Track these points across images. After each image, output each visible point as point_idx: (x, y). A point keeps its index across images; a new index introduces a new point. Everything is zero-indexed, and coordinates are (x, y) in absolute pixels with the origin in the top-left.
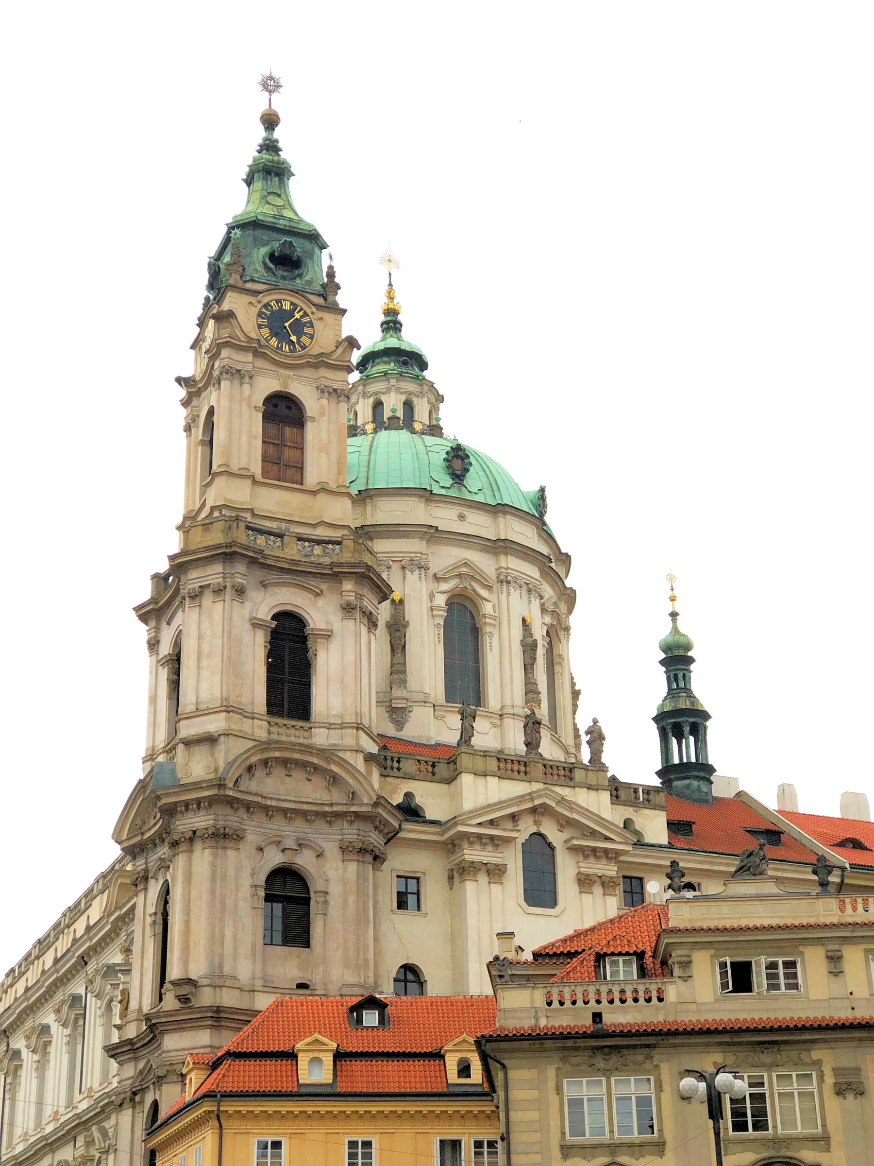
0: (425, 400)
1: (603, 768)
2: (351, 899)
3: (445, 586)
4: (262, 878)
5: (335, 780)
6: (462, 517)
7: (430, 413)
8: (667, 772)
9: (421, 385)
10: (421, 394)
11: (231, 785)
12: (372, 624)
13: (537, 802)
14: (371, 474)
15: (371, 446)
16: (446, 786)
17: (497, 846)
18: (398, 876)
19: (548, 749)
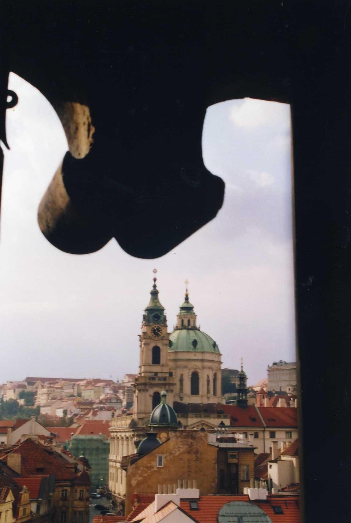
10: (192, 318)
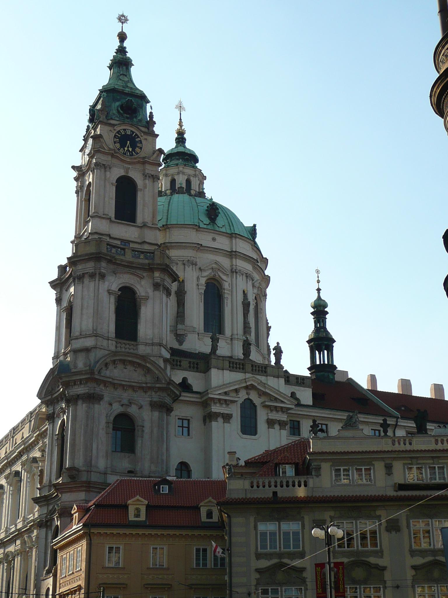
0: (197, 178)
1: (282, 367)
2: (155, 430)
3: (205, 274)
4: (112, 418)
5: (149, 370)
6: (214, 239)
7: (199, 184)
8: (313, 368)
9: (195, 171)
10: (195, 176)
11: (96, 373)
12: (169, 294)
13: (248, 384)
14: (169, 217)
15: (169, 202)
16: (204, 375)
17: (228, 405)
18: (178, 419)
19: (255, 356)
